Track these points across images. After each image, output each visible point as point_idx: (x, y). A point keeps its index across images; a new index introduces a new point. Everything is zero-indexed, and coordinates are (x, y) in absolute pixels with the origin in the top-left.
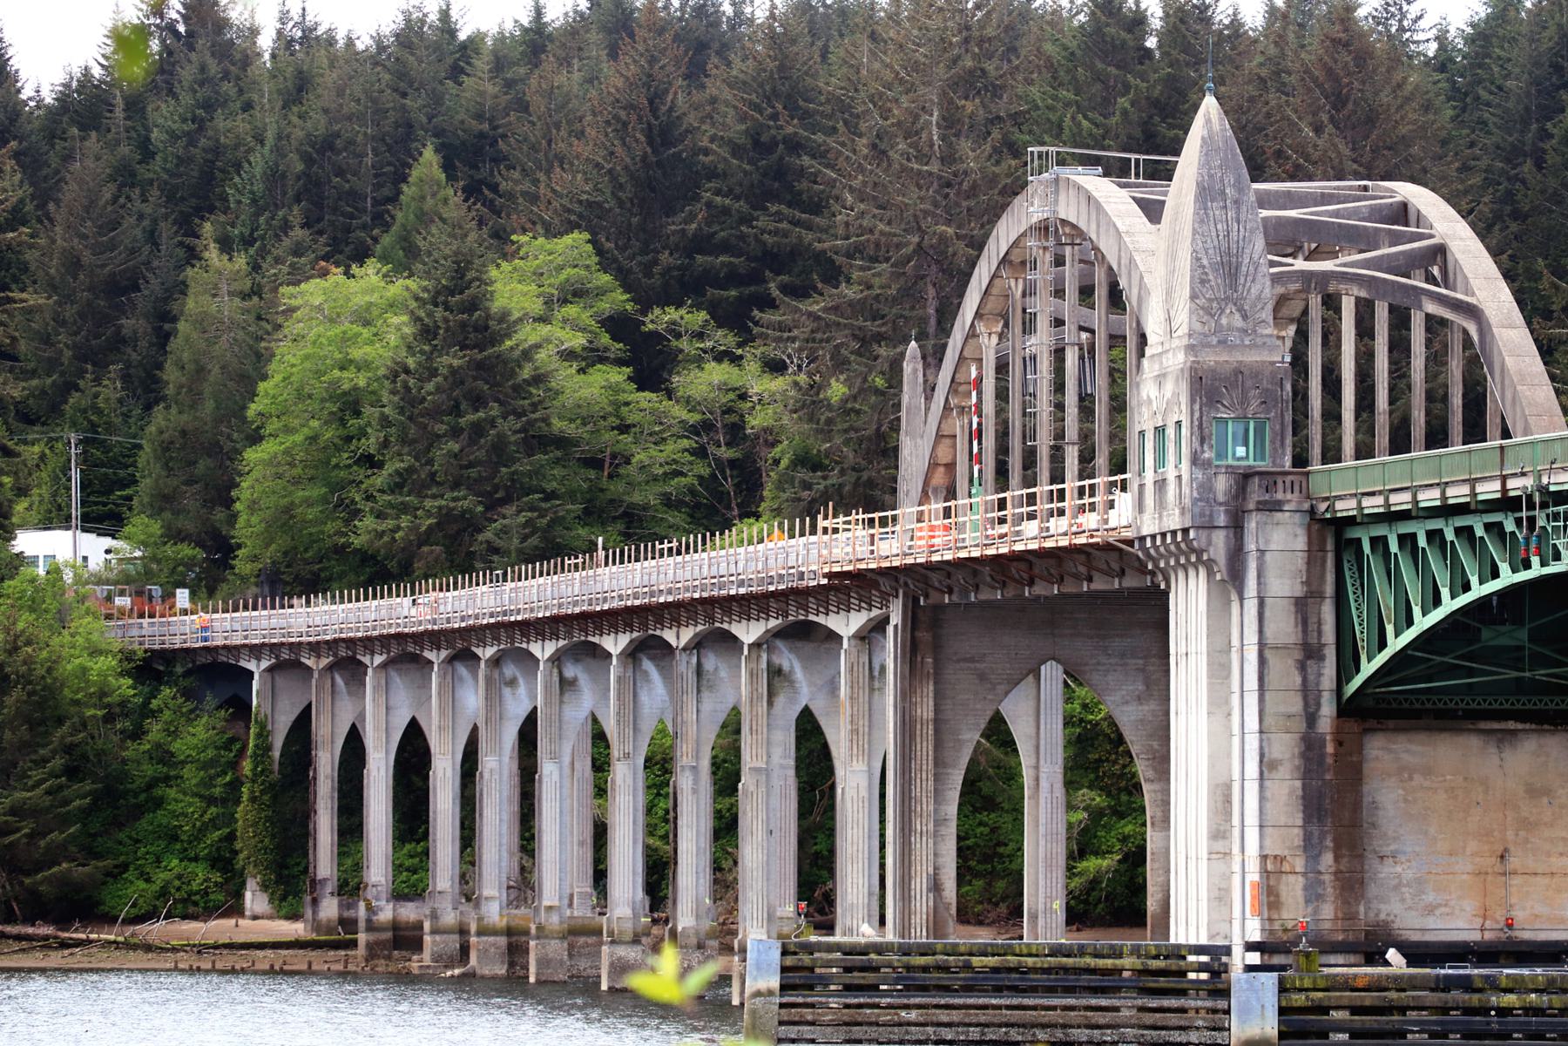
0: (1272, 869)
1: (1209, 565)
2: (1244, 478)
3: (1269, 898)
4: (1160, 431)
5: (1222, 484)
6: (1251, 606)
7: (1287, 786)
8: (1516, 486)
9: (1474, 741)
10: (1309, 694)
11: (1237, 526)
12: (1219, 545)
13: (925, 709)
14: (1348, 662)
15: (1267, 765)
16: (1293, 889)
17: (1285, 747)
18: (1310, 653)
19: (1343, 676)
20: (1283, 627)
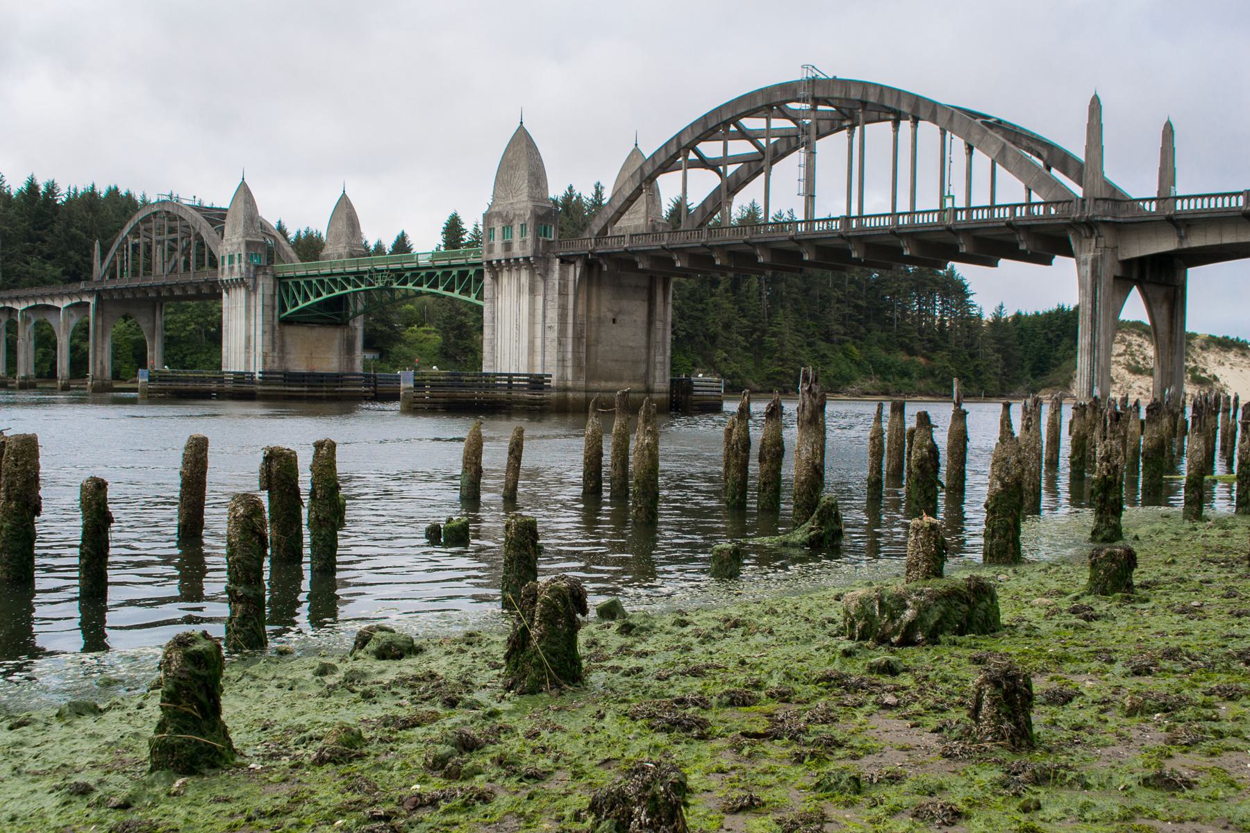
0: (265, 356)
1: (247, 287)
2: (258, 267)
3: (265, 362)
4: (231, 258)
5: (252, 268)
6: (259, 297)
7: (268, 336)
8: (361, 269)
9: (306, 329)
10: (273, 316)
11: (255, 278)
12: (251, 282)
13: (100, 323)
14: (283, 309)
15: (264, 332)
16: (269, 359)
17: (268, 328)
18: (274, 308)
19: (280, 313)
20: (268, 301)
